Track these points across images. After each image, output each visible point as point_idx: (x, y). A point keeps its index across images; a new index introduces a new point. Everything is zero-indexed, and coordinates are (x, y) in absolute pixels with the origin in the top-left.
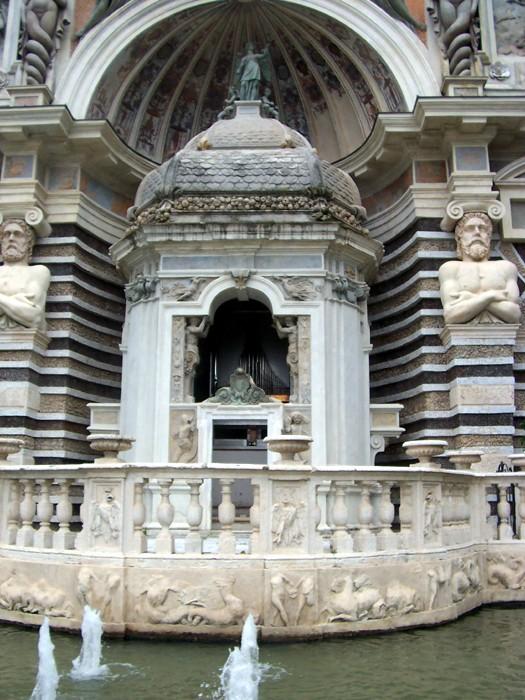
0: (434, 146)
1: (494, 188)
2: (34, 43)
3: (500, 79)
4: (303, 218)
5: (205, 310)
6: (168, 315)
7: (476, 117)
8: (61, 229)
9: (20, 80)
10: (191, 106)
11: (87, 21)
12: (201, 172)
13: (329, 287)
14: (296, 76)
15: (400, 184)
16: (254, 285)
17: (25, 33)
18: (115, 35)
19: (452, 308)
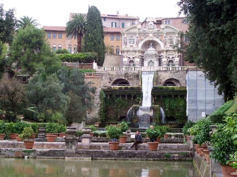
0: (163, 51)
1: (166, 54)
8: (139, 56)
12: (149, 53)
15: (161, 52)
19: (163, 61)
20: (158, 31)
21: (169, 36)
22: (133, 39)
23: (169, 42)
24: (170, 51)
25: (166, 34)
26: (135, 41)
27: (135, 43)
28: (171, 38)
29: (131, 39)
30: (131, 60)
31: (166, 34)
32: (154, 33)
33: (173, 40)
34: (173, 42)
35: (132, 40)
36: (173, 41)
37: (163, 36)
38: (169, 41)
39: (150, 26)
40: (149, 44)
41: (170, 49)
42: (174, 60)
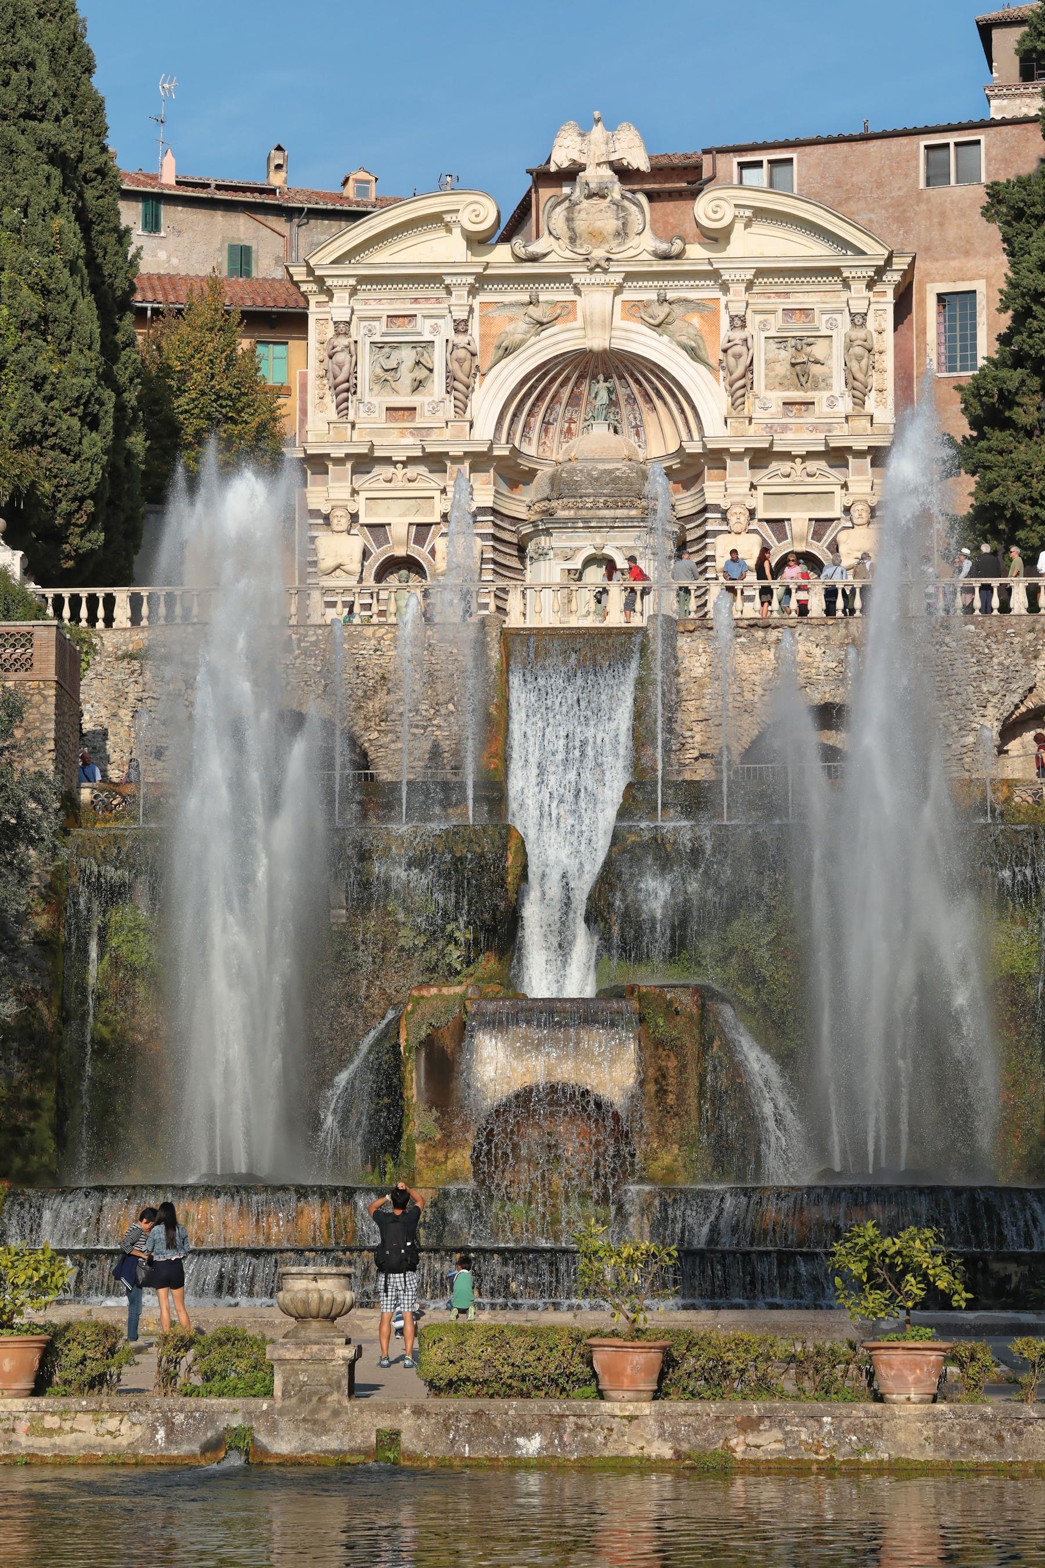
1: (753, 487)
2: (457, 384)
3: (766, 409)
4: (633, 513)
5: (579, 566)
6: (558, 569)
7: (738, 447)
8: (482, 510)
9: (448, 409)
10: (557, 407)
11: (489, 364)
13: (649, 551)
14: (634, 387)
16: (605, 551)
17: (450, 376)
18: (510, 374)
20: (666, 257)
21: (780, 304)
22: (414, 345)
23: (783, 369)
24: (788, 456)
25: (750, 285)
26: (438, 359)
27: (438, 382)
28: (797, 328)
29: (396, 346)
30: (400, 552)
31: (750, 285)
32: (629, 276)
33: (818, 350)
34: (815, 369)
35: (408, 356)
36: (817, 362)
37: (716, 313)
38: (786, 355)
39: (586, 203)
40: (574, 400)
41: (789, 435)
42: (834, 547)
